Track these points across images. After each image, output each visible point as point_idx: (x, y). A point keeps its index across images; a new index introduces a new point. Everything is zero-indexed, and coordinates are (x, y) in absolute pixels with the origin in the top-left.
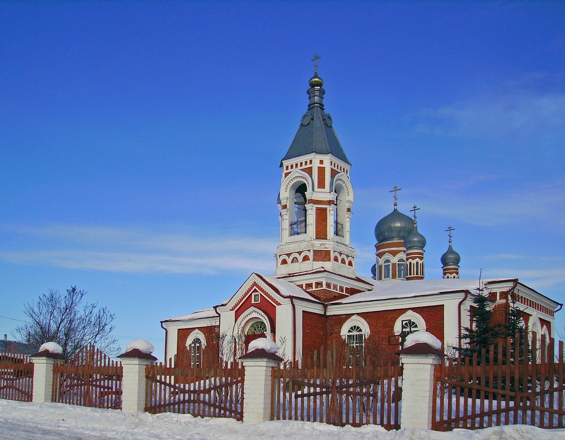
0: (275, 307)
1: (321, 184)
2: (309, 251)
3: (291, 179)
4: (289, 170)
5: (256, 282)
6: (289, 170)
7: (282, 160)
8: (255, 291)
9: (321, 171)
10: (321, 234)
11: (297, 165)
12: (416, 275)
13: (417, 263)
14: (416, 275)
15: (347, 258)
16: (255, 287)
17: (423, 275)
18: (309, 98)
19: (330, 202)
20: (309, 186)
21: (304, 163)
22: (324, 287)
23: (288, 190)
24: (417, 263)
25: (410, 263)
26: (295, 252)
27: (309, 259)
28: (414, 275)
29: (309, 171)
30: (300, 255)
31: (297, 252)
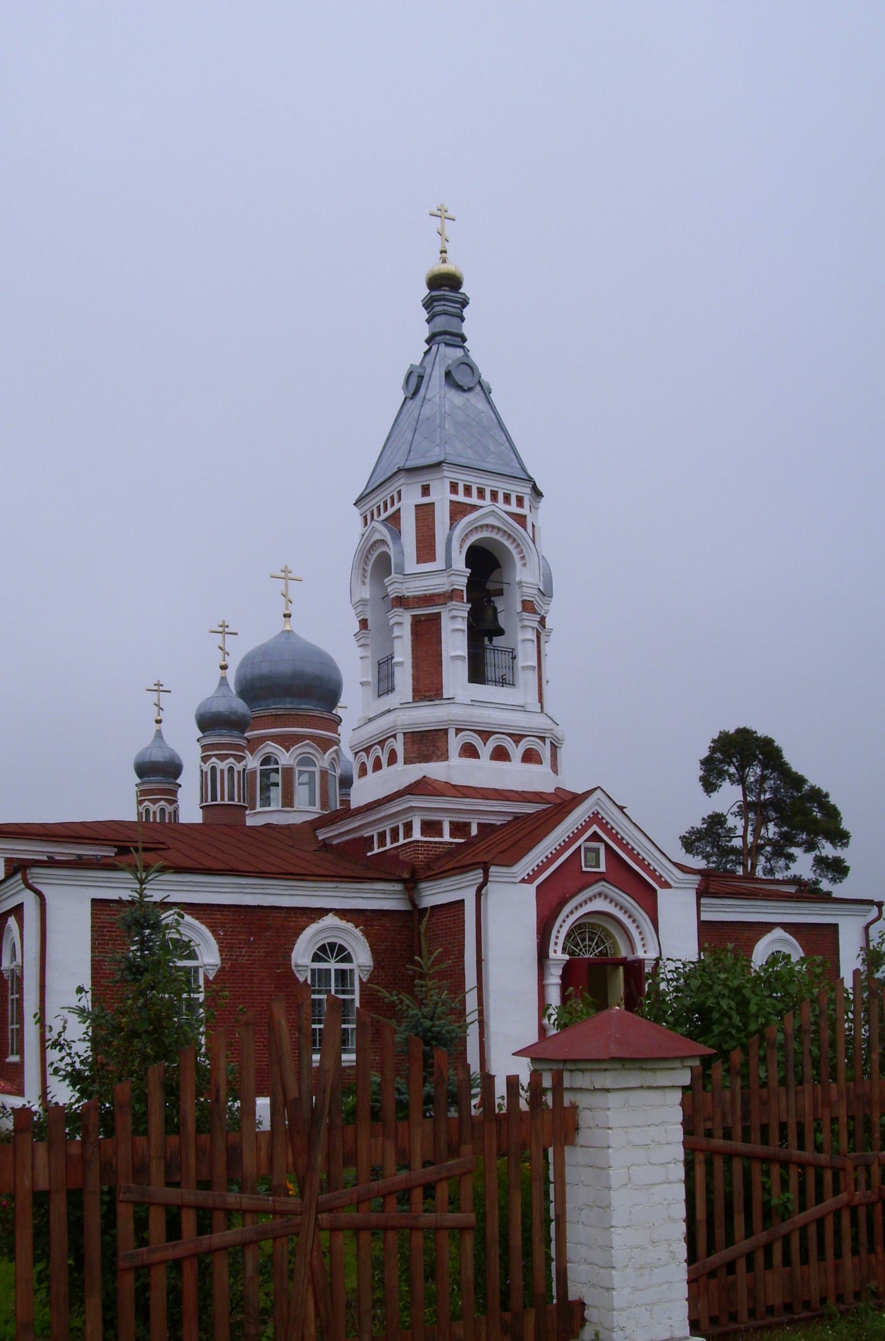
0: (655, 891)
2: (543, 739)
5: (598, 813)
6: (461, 498)
12: (212, 801)
14: (212, 801)
16: (595, 828)
20: (524, 565)
26: (503, 733)
31: (510, 735)
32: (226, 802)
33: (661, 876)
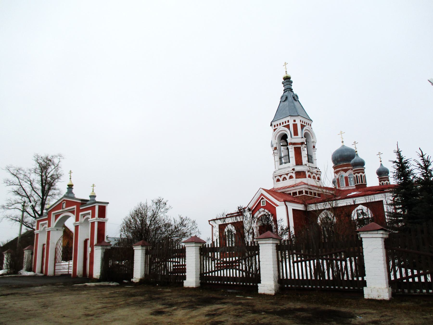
0: (275, 208)
1: (296, 133)
3: (278, 132)
4: (276, 127)
6: (276, 127)
7: (272, 122)
8: (262, 199)
9: (295, 126)
10: (299, 162)
11: (280, 124)
13: (361, 176)
15: (317, 175)
16: (262, 196)
17: (366, 183)
18: (284, 86)
19: (302, 143)
21: (284, 123)
22: (304, 194)
23: (277, 139)
24: (361, 176)
25: (357, 176)
27: (293, 178)
28: (360, 183)
29: (288, 126)
30: (287, 175)
31: (286, 174)
32: (361, 183)
33: (276, 204)
